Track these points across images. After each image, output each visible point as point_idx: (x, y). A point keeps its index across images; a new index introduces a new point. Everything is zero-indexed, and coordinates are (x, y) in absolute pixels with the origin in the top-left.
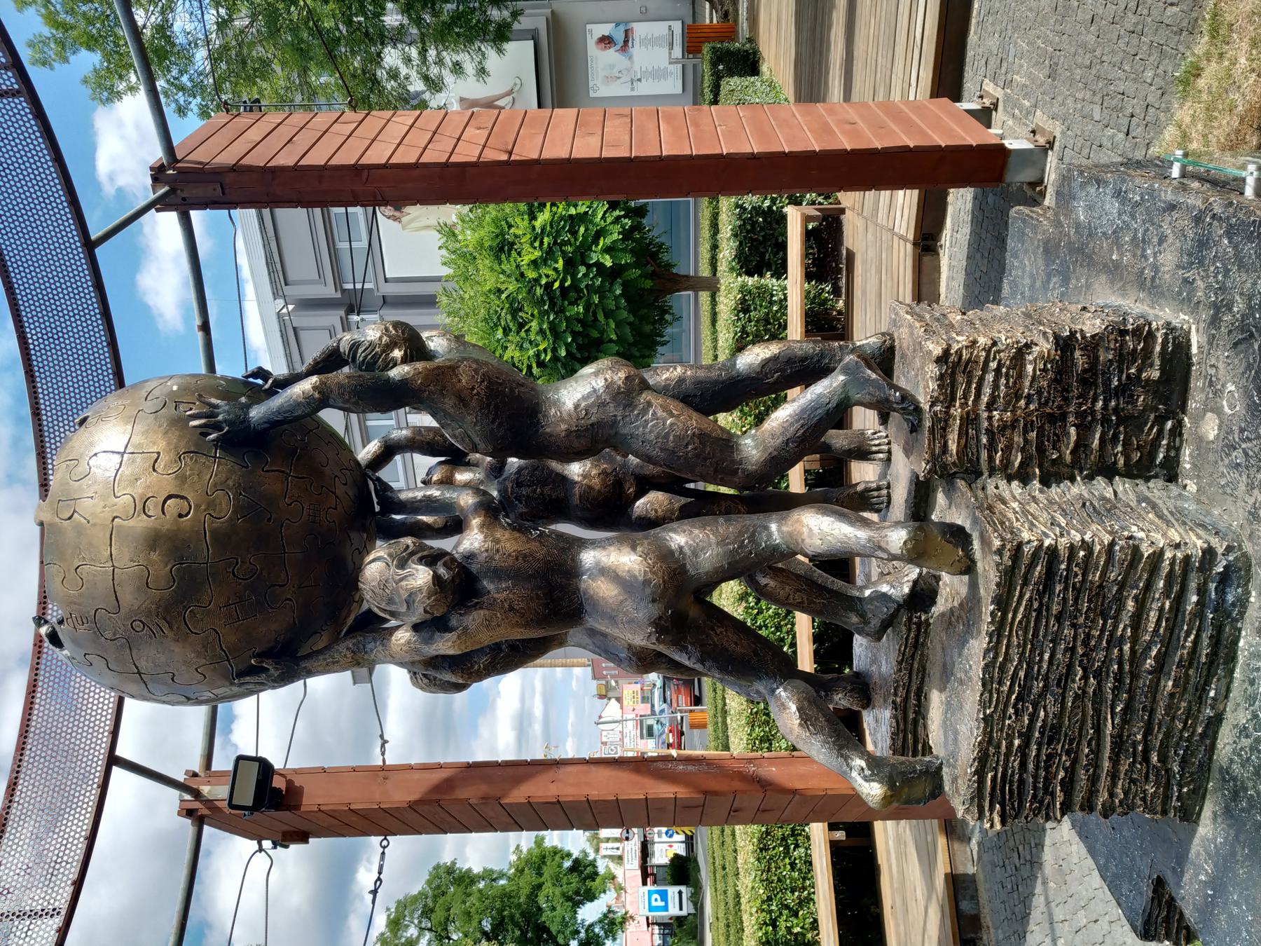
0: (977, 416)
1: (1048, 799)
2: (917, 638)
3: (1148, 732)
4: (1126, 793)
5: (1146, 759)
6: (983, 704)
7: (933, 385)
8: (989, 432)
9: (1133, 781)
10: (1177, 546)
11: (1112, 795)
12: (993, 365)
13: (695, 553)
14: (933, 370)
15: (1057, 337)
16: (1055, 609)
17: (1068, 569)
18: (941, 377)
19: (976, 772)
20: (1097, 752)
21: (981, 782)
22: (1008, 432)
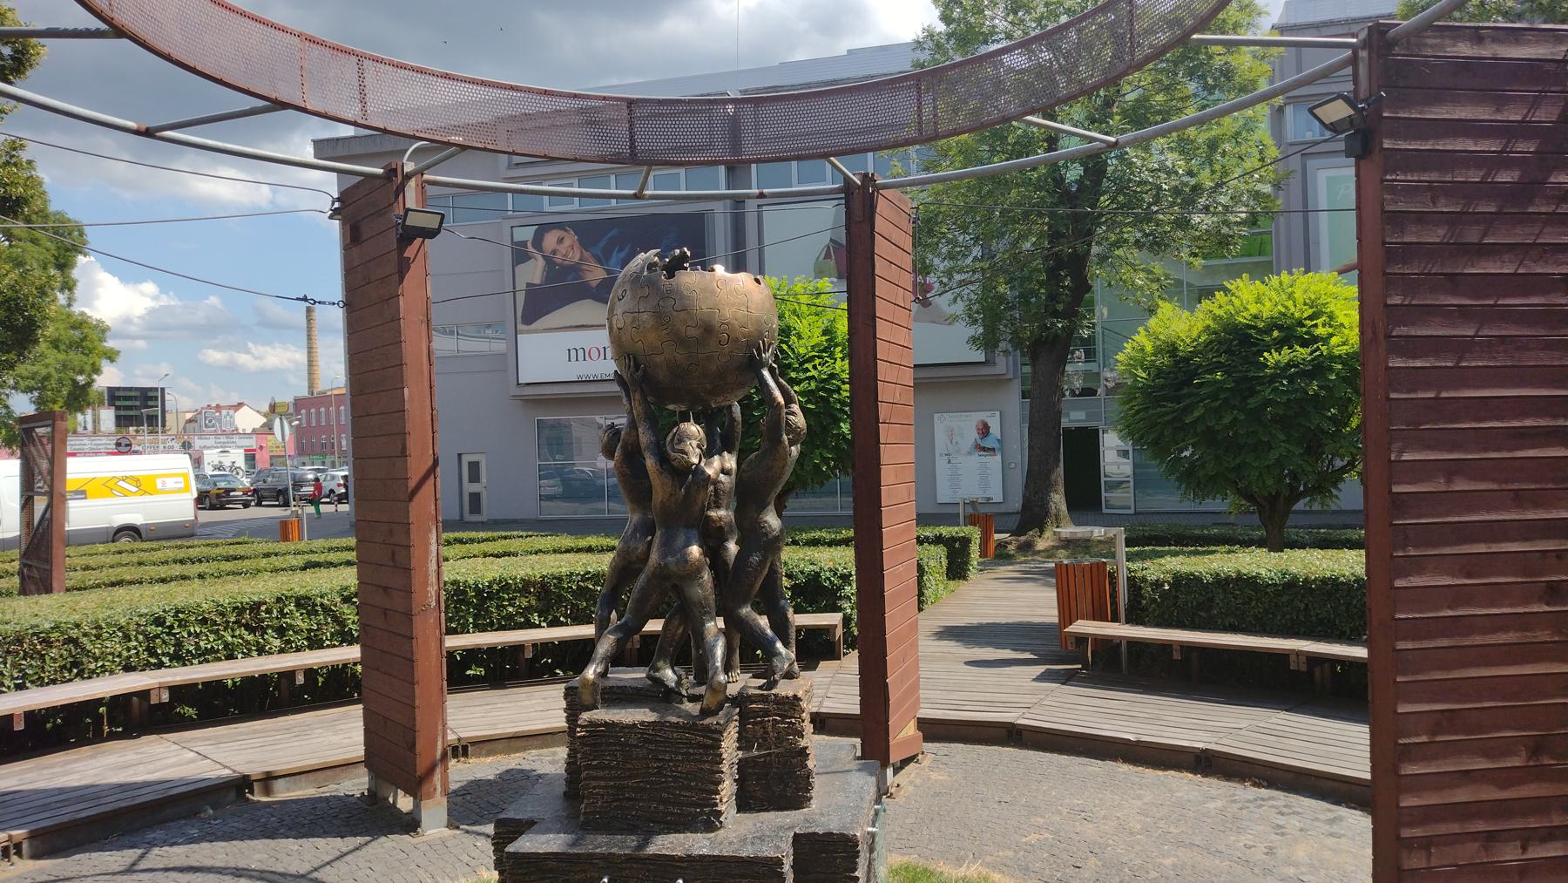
0: (769, 716)
1: (591, 758)
2: (650, 696)
3: (629, 799)
4: (597, 794)
5: (616, 801)
6: (642, 723)
7: (784, 694)
8: (761, 722)
9: (603, 796)
10: (721, 801)
11: (594, 788)
12: (793, 720)
13: (700, 585)
14: (791, 694)
15: (807, 748)
16: (690, 750)
17: (710, 754)
18: (787, 697)
19: (606, 722)
20: (619, 778)
21: (601, 725)
22: (762, 730)
